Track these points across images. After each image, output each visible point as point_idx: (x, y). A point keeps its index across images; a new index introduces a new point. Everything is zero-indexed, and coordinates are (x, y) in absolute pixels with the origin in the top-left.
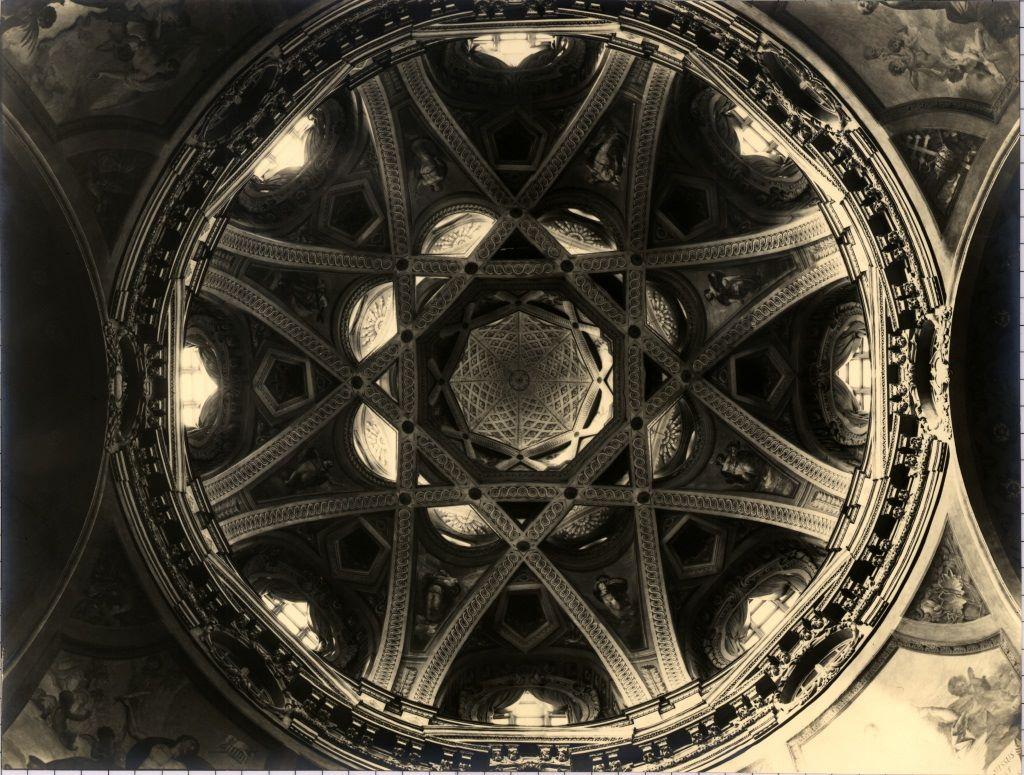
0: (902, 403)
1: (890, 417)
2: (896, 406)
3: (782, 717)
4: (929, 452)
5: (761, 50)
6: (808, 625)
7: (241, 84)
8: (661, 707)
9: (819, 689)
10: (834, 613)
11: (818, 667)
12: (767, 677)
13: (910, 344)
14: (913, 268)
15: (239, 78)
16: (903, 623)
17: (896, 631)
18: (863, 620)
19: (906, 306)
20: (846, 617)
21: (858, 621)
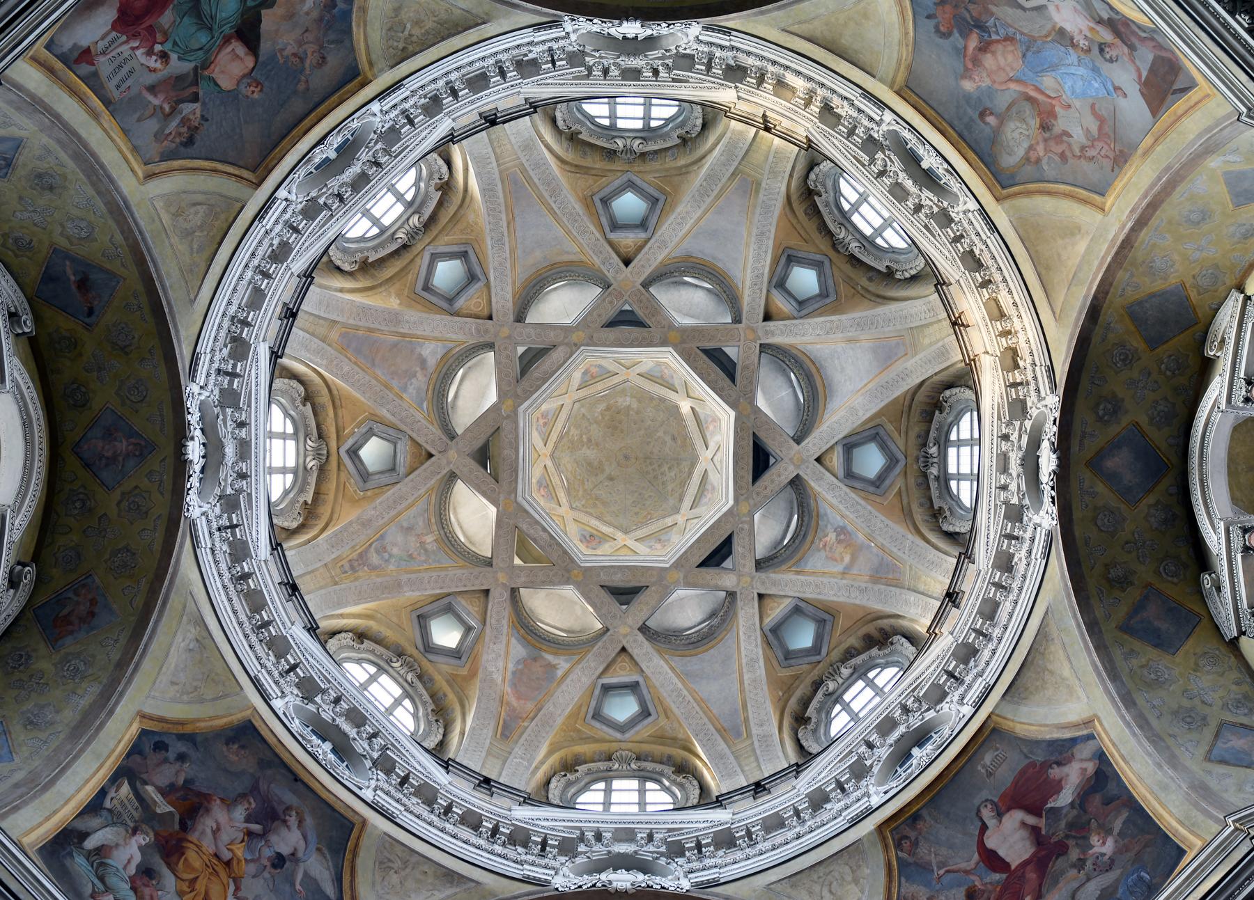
1: (674, 80)
2: (663, 74)
3: (972, 205)
4: (711, 44)
5: (293, 197)
6: (882, 173)
7: (310, 741)
9: (946, 165)
10: (871, 144)
11: (925, 165)
12: (931, 215)
14: (524, 50)
15: (304, 742)
17: (891, 87)
18: (878, 118)
19: (562, 60)
20: (876, 135)
21: (879, 124)
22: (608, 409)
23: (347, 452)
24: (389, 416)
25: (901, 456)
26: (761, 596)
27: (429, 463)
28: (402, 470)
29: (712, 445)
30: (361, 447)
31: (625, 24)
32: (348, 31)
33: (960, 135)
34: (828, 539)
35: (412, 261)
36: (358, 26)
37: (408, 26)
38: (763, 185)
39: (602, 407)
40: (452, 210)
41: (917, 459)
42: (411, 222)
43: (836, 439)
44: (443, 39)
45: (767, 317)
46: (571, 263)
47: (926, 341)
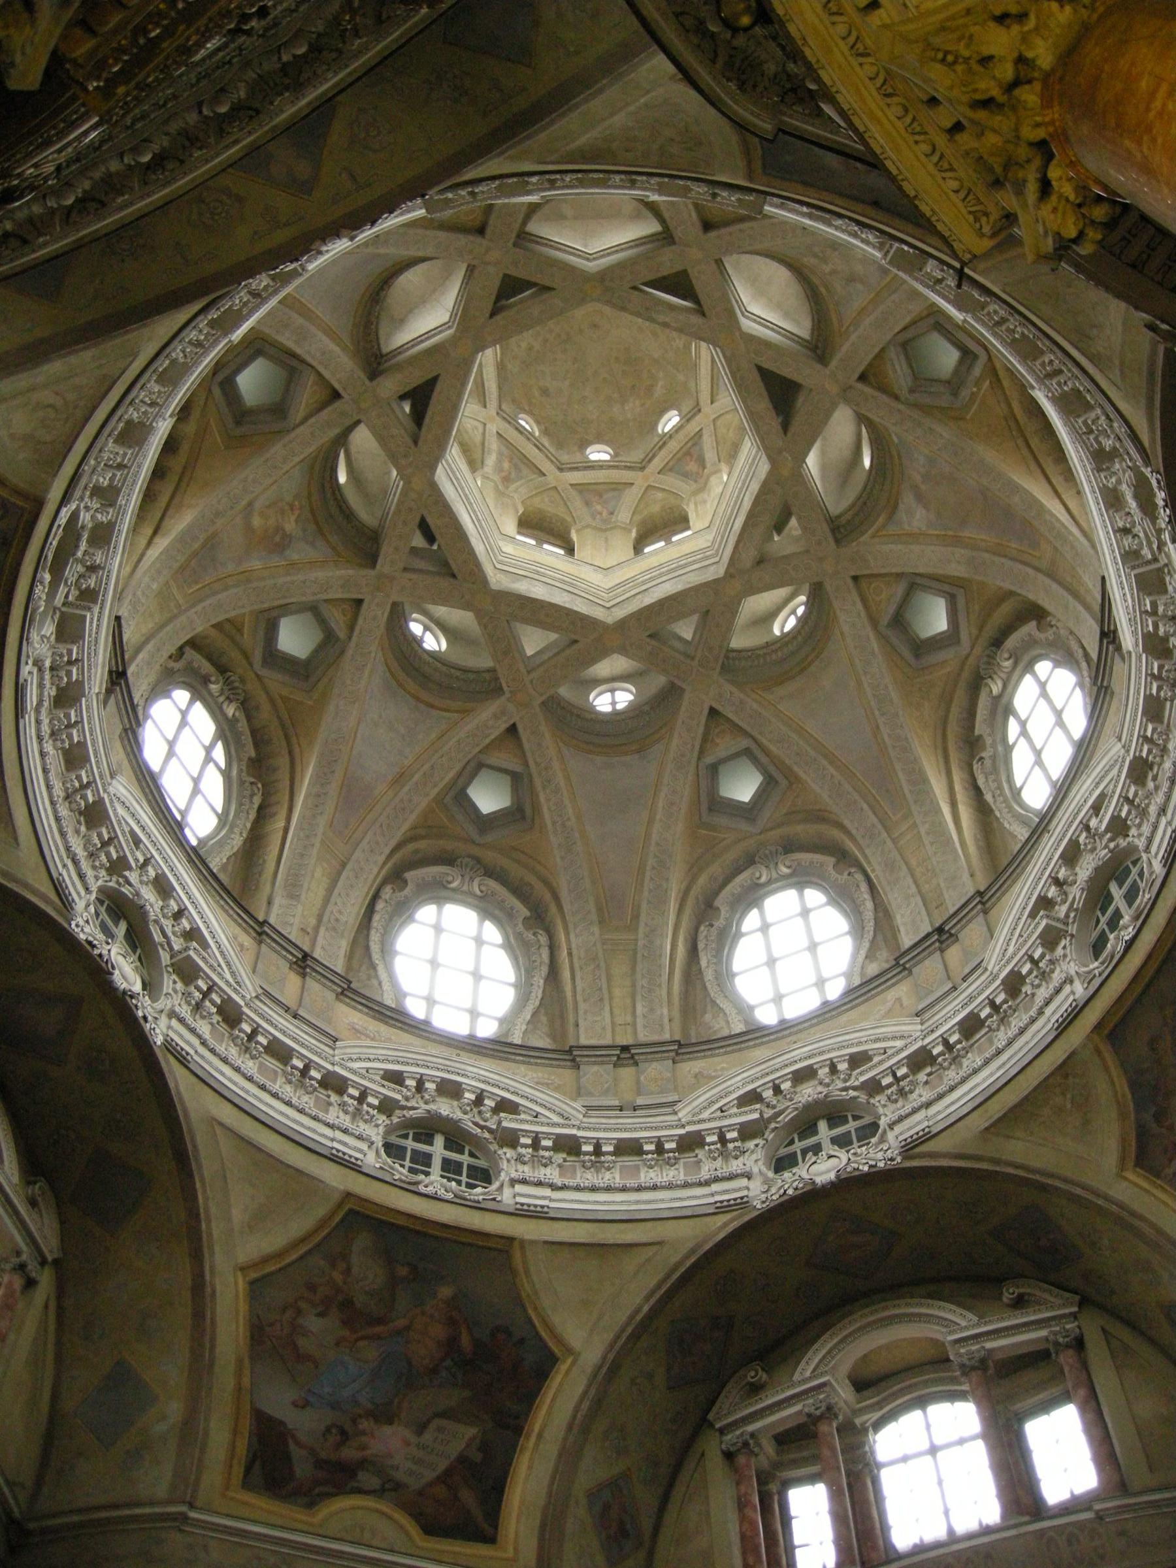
0: (775, 1102)
8: (295, 963)
13: (846, 1089)
16: (533, 1242)
22: (650, 389)
23: (976, 357)
24: (939, 428)
25: (264, 672)
26: (336, 395)
27: (861, 368)
28: (892, 353)
29: (493, 444)
30: (961, 362)
31: (832, 1176)
32: (1134, 1085)
33: (425, 1235)
34: (293, 518)
35: (981, 629)
36: (1124, 1096)
37: (1069, 1106)
38: (596, 929)
39: (659, 391)
40: (955, 713)
41: (242, 680)
42: (1000, 684)
43: (353, 644)
44: (1026, 1098)
45: (512, 730)
46: (782, 679)
47: (318, 873)
